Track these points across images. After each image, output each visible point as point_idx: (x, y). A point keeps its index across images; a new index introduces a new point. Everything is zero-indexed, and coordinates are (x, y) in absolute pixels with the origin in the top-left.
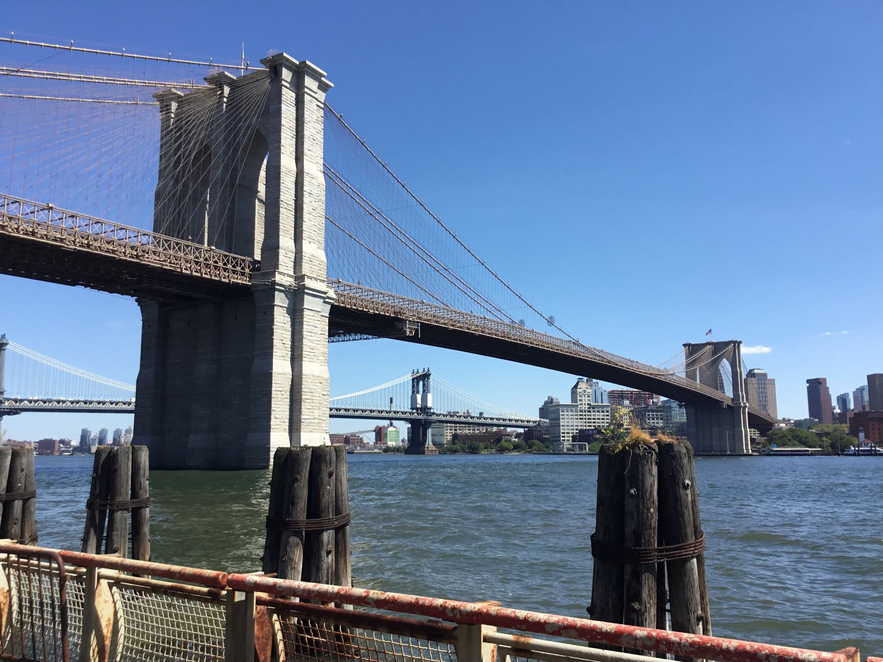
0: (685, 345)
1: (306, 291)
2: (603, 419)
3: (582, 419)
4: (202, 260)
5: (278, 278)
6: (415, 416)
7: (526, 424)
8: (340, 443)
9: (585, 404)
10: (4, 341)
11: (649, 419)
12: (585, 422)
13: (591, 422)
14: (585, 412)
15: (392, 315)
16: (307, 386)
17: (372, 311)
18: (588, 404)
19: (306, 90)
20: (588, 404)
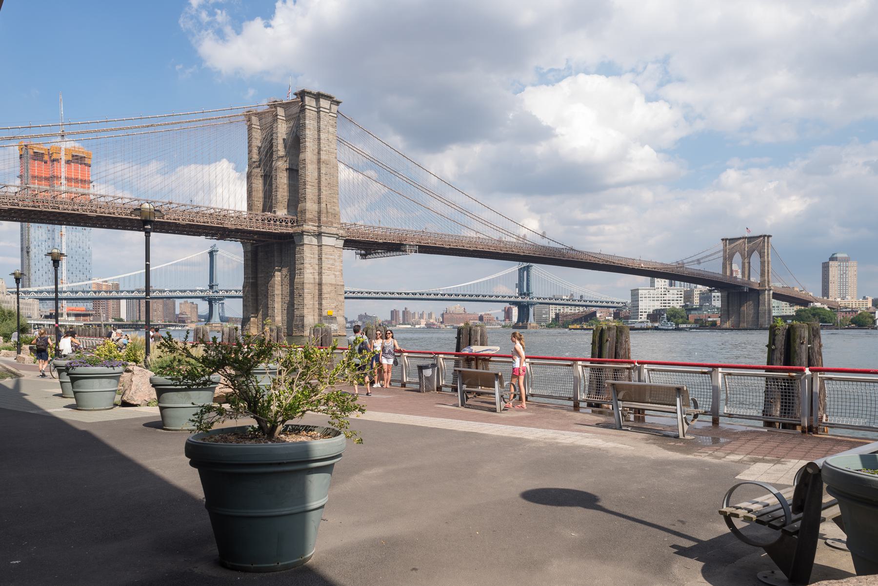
0: (723, 240)
1: (323, 234)
2: (676, 300)
3: (658, 300)
4: (260, 221)
5: (306, 227)
6: (520, 299)
7: (615, 305)
8: (475, 320)
9: (661, 288)
10: (216, 249)
11: (714, 300)
12: (661, 303)
13: (666, 303)
14: (661, 294)
15: (397, 242)
16: (325, 289)
17: (381, 241)
18: (664, 288)
19: (321, 109)
20: (664, 288)
